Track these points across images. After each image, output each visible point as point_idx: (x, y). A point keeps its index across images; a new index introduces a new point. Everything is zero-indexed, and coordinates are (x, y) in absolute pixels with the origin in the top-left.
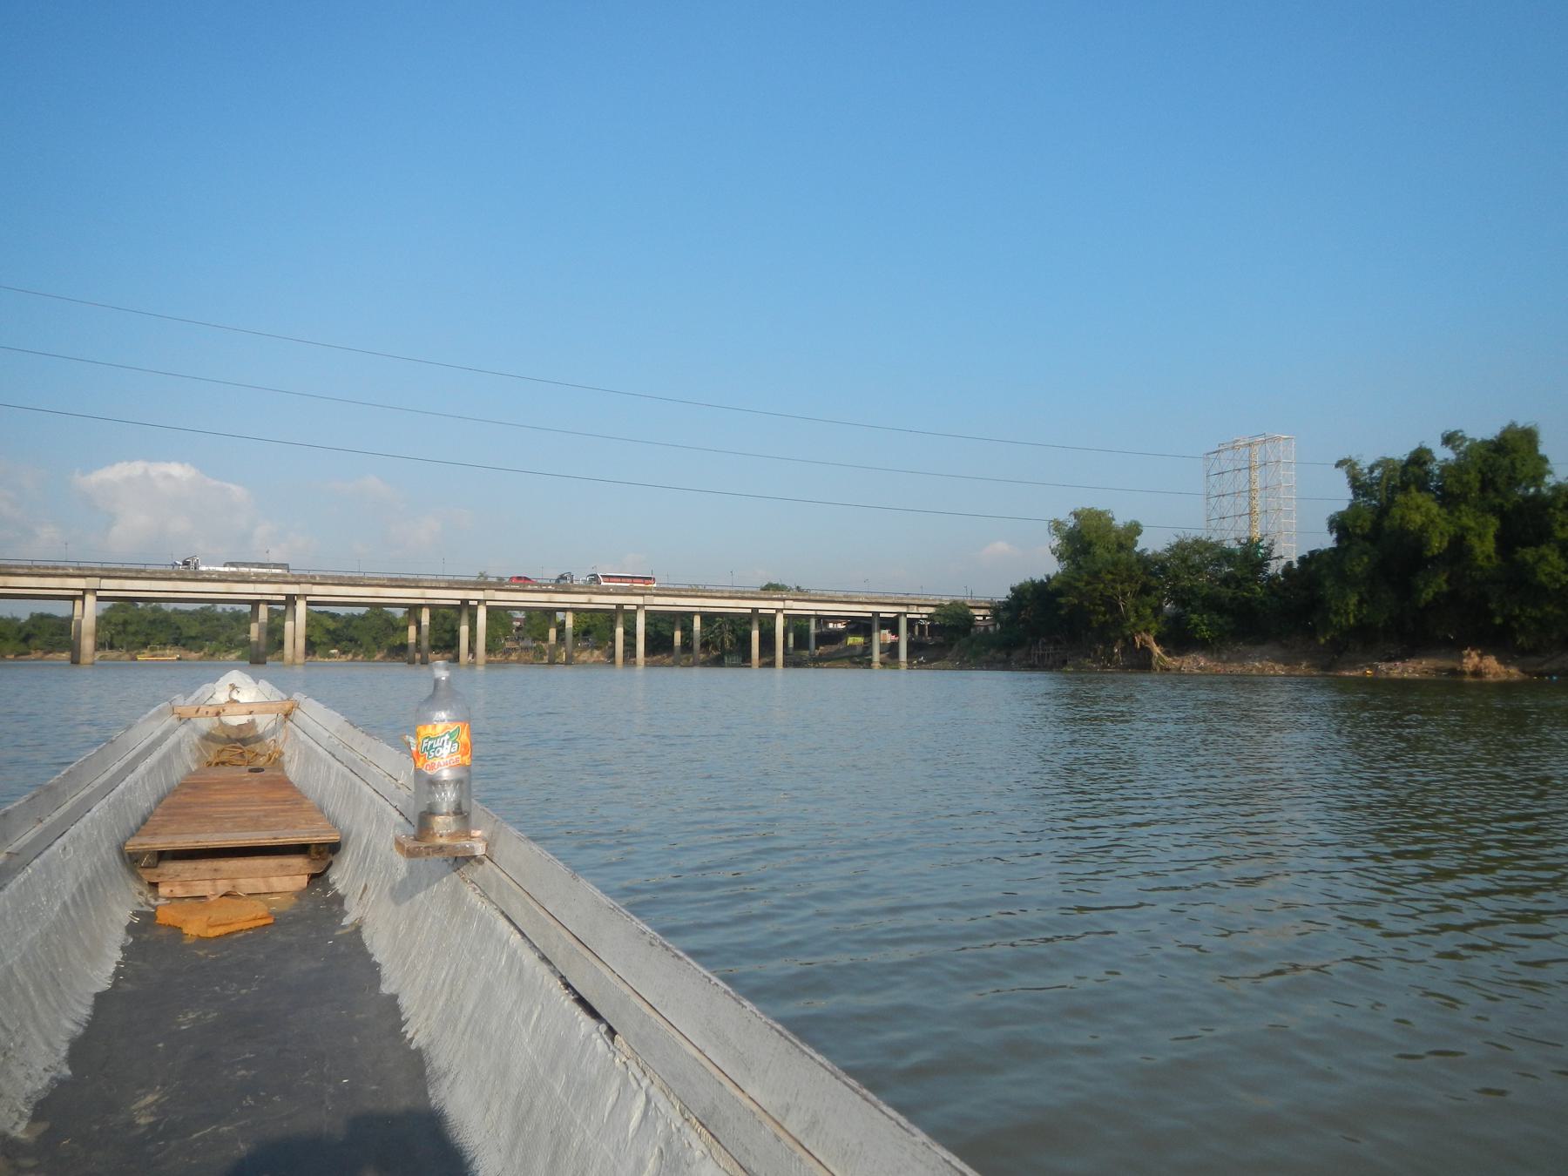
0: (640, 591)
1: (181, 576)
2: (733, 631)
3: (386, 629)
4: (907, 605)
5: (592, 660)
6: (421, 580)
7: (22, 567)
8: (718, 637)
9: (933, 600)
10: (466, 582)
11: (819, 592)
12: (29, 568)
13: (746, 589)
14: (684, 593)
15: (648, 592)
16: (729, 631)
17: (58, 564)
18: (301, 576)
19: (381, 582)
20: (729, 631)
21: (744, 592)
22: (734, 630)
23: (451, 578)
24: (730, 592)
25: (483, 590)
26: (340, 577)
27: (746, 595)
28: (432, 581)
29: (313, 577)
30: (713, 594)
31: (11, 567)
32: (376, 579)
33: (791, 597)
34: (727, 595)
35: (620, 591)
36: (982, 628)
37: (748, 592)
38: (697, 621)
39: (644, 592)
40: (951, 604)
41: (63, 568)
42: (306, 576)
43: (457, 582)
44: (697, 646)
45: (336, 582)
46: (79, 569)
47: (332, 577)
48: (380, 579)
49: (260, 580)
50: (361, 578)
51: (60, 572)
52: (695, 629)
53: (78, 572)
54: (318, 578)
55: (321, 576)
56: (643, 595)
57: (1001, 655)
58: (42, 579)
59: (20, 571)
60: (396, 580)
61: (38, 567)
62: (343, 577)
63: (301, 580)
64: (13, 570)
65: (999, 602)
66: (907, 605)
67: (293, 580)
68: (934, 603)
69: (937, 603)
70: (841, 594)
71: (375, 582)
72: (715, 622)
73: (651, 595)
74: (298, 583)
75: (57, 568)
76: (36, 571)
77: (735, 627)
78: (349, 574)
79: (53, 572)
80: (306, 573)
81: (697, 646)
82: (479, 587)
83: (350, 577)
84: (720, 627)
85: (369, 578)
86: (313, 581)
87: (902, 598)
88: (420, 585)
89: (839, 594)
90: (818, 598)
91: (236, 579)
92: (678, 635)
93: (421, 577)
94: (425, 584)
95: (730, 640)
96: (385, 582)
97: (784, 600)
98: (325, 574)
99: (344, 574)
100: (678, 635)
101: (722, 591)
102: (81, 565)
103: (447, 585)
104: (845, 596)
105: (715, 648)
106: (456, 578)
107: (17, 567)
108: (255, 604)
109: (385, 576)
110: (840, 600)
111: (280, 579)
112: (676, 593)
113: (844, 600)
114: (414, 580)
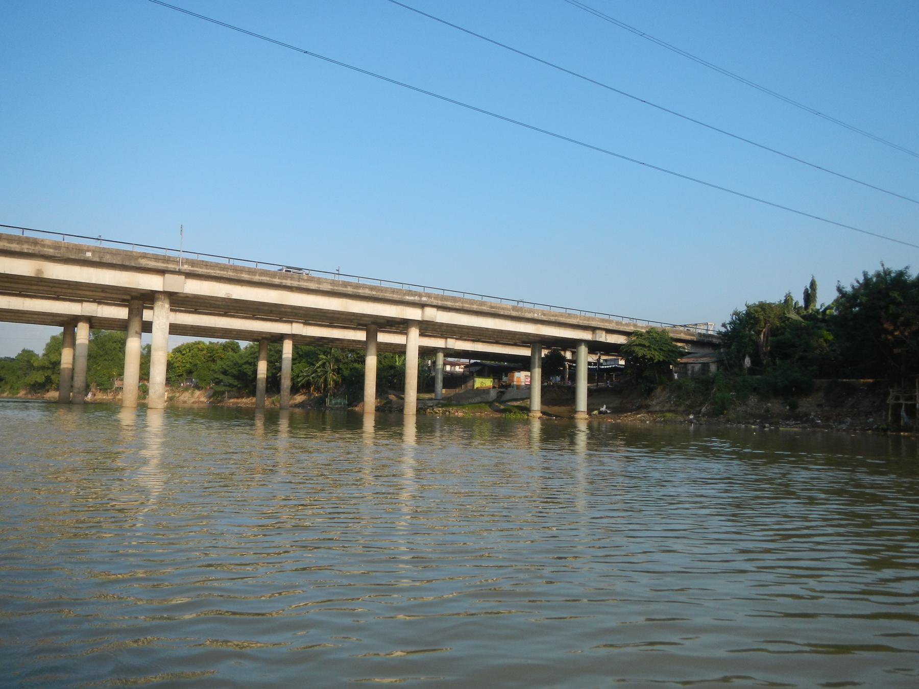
0: (152, 264)
2: (338, 371)
3: (27, 369)
4: (594, 329)
5: (192, 400)
8: (320, 377)
9: (626, 324)
11: (479, 298)
13: (362, 281)
14: (245, 276)
15: (171, 266)
16: (333, 370)
20: (333, 370)
21: (357, 286)
22: (339, 369)
24: (333, 283)
27: (361, 291)
30: (304, 284)
33: (435, 302)
34: (326, 287)
35: (108, 259)
36: (697, 367)
37: (364, 286)
38: (288, 348)
39: (160, 265)
40: (647, 332)
44: (286, 383)
52: (284, 356)
56: (162, 272)
57: (775, 406)
65: (699, 334)
66: (594, 329)
68: (621, 328)
69: (631, 329)
70: (509, 304)
72: (318, 360)
73: (179, 273)
77: (341, 366)
81: (286, 383)
84: (324, 365)
87: (589, 319)
89: (505, 304)
90: (475, 307)
92: (262, 368)
95: (334, 381)
97: (422, 306)
100: (262, 368)
101: (319, 281)
104: (514, 308)
105: (318, 389)
110: (506, 313)
112: (231, 274)
113: (514, 314)
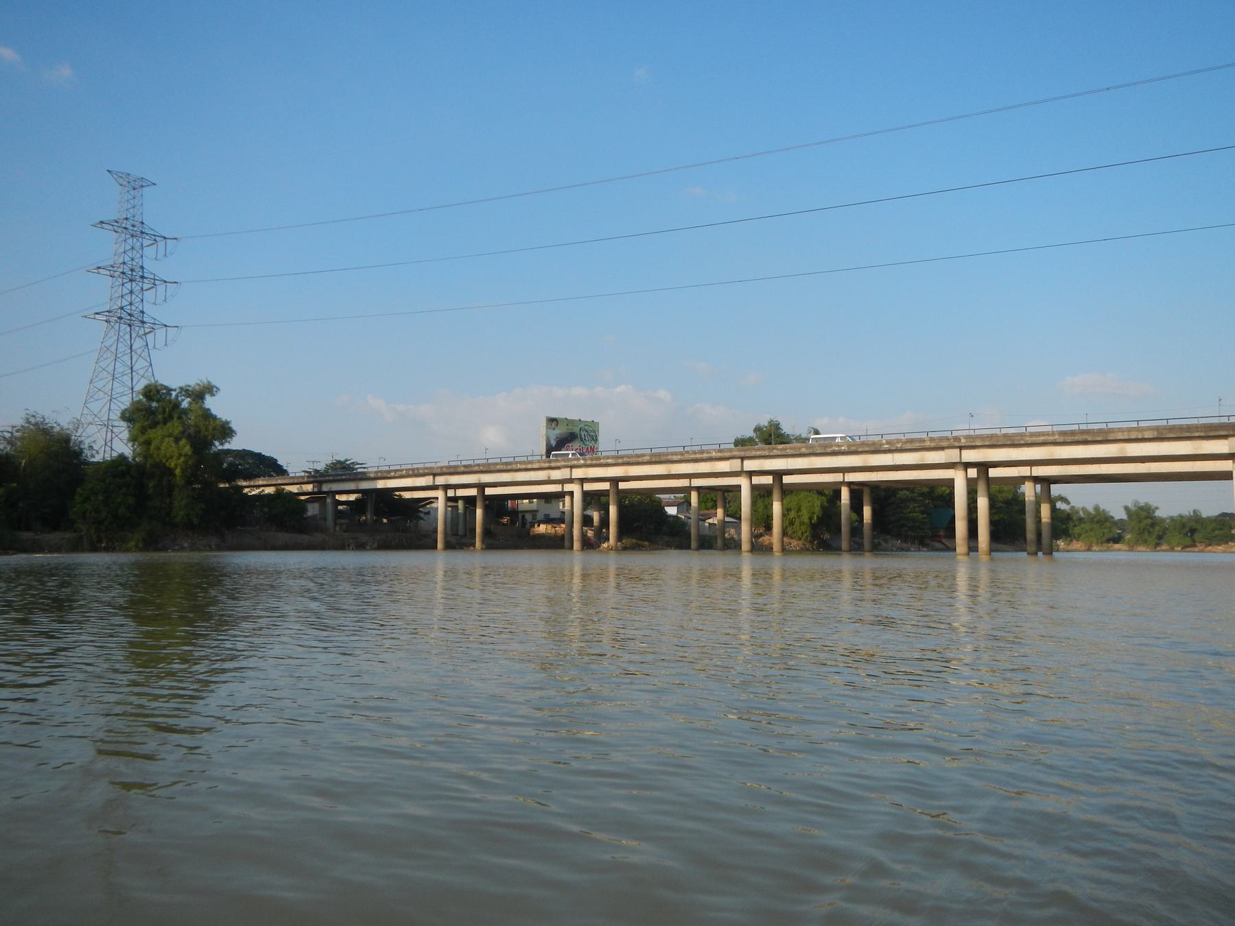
1: (811, 451)
6: (1111, 431)
7: (676, 454)
10: (1189, 428)
12: (682, 454)
17: (704, 448)
18: (941, 439)
19: (1051, 438)
23: (1164, 423)
25: (1225, 437)
26: (991, 437)
28: (1130, 430)
29: (957, 439)
31: (667, 454)
32: (1043, 434)
41: (708, 452)
42: (947, 439)
43: (1172, 429)
45: (987, 443)
46: (720, 451)
47: (982, 437)
48: (1047, 434)
49: (893, 448)
50: (1021, 435)
51: (705, 455)
53: (719, 455)
54: (963, 441)
55: (967, 437)
58: (696, 464)
59: (675, 458)
60: (1073, 433)
61: (687, 452)
62: (996, 436)
63: (944, 444)
64: (670, 457)
67: (933, 445)
71: (1042, 439)
74: (942, 448)
75: (702, 452)
76: (687, 456)
78: (1004, 431)
79: (698, 456)
80: (948, 434)
82: (1212, 434)
83: (1005, 435)
85: (1032, 435)
86: (956, 444)
88: (1111, 438)
91: (867, 449)
93: (1111, 426)
94: (1120, 436)
96: (1057, 437)
98: (972, 433)
99: (997, 432)
102: (722, 447)
103: (1155, 434)
106: (1171, 423)
107: (672, 454)
108: (1046, 481)
109: (1055, 428)
111: (917, 445)
114: (1100, 431)
